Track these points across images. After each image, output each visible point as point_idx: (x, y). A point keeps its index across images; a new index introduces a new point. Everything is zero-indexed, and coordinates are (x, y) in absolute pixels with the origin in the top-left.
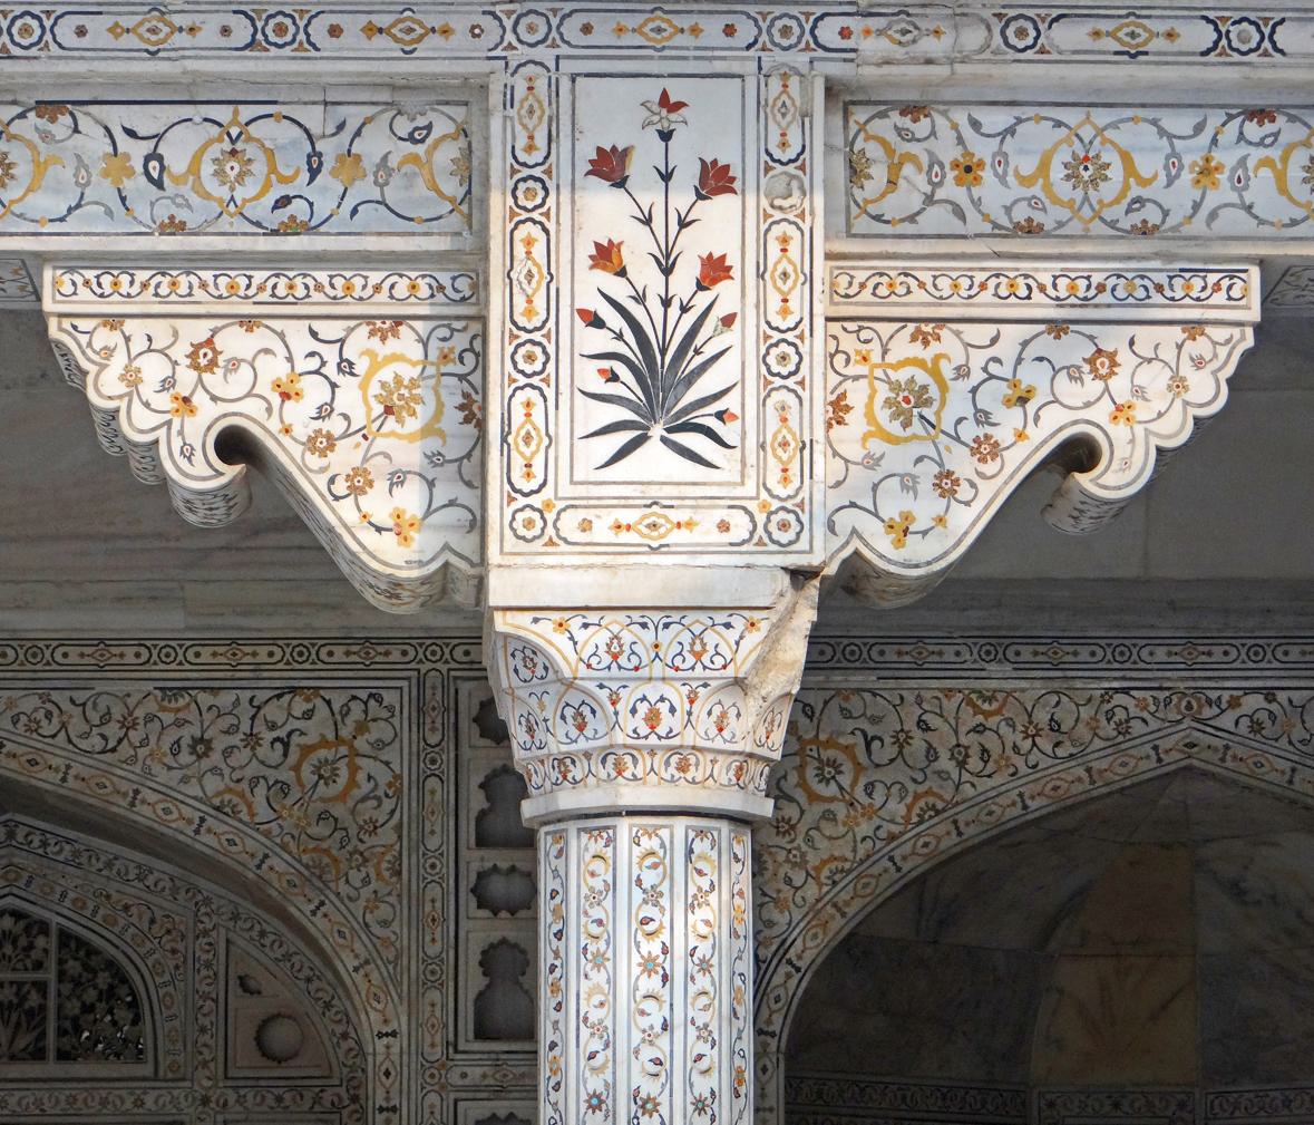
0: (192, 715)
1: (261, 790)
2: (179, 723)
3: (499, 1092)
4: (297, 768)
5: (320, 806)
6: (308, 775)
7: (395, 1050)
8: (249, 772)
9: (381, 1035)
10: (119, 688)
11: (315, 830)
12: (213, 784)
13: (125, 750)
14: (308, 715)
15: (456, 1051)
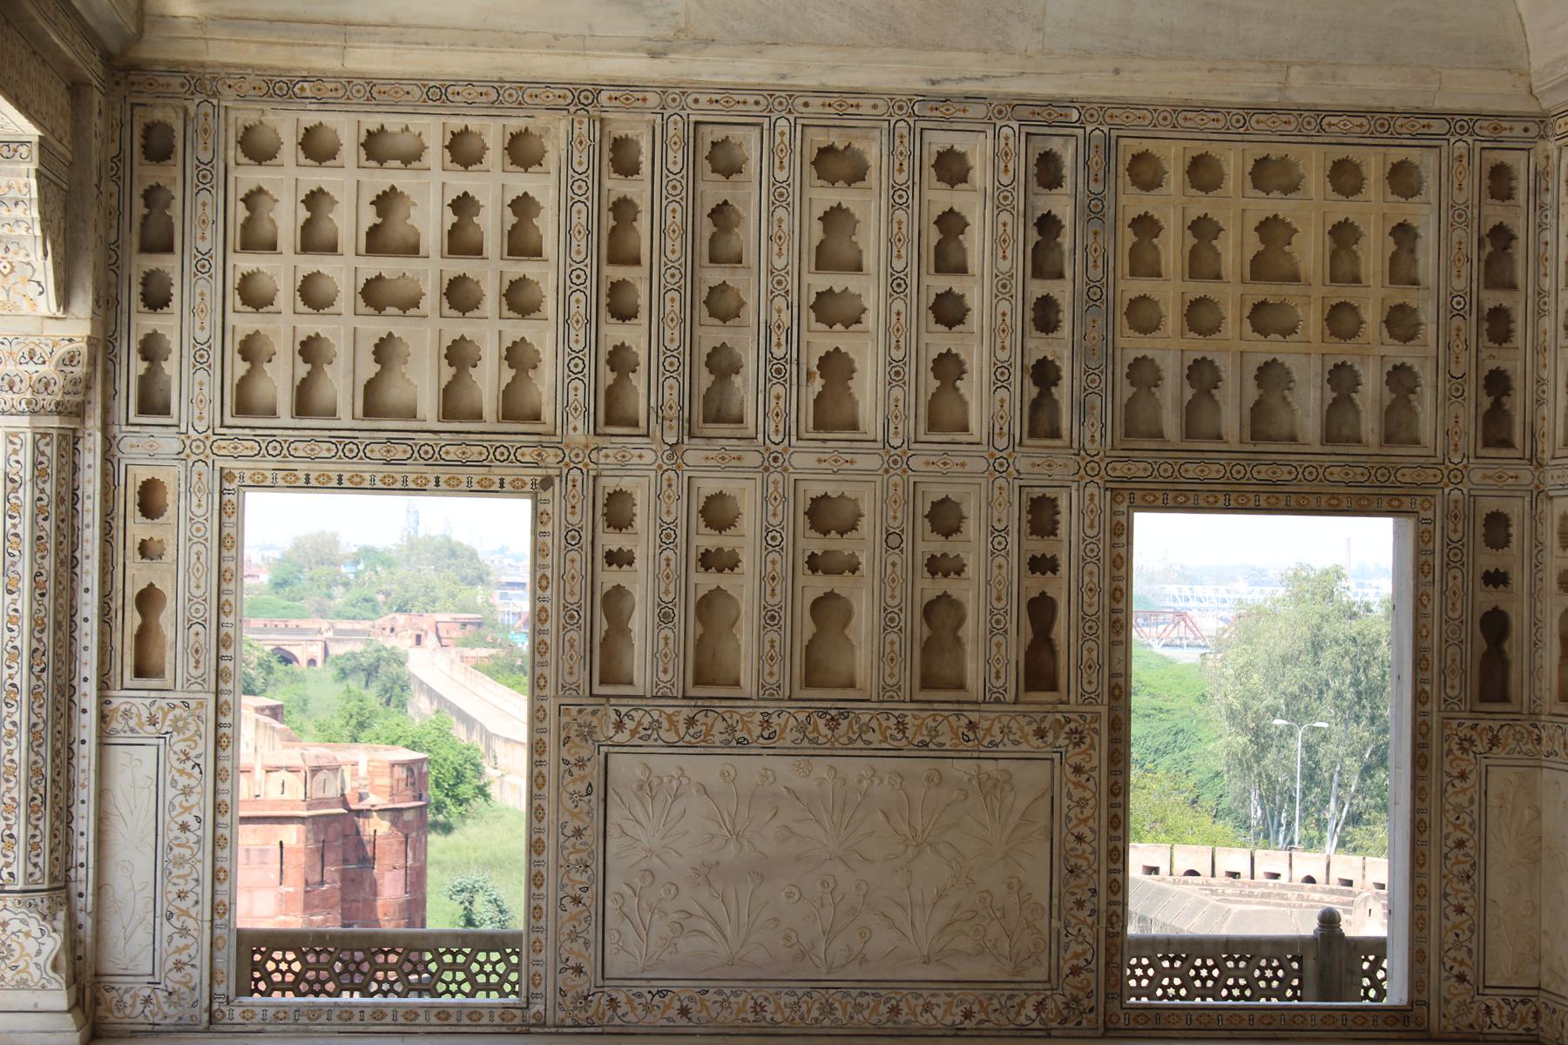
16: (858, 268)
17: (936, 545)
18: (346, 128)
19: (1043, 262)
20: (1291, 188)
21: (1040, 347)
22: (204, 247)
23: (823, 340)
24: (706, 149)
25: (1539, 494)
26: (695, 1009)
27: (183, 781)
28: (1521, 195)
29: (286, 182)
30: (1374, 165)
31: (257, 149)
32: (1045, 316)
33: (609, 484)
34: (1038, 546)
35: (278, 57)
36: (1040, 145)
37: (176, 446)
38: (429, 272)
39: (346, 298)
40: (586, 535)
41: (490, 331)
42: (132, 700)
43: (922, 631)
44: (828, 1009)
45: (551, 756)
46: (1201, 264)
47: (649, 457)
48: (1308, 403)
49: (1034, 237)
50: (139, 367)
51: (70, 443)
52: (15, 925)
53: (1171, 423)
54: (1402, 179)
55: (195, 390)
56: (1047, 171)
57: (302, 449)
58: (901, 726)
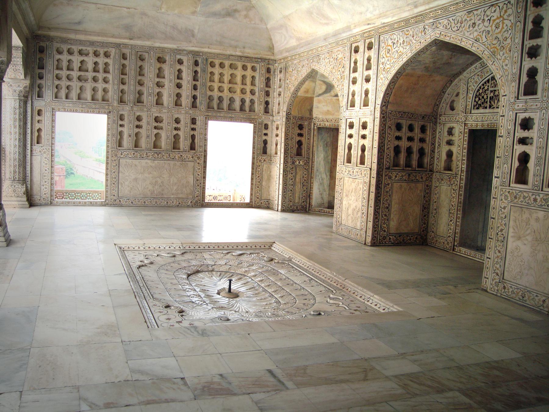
0: (473, 18)
1: (484, 34)
2: (470, 20)
3: (525, 110)
4: (491, 26)
5: (496, 35)
6: (494, 28)
7: (506, 100)
8: (482, 30)
9: (503, 96)
10: (459, 14)
11: (494, 42)
12: (476, 34)
13: (461, 29)
14: (495, 11)
15: (518, 99)
16: (164, 78)
17: (176, 125)
18: (75, 48)
19: (195, 79)
20: (236, 69)
21: (194, 93)
22: (50, 68)
23: (157, 90)
24: (139, 56)
25: (273, 121)
26: (134, 202)
27: (46, 162)
28: (272, 73)
29: (65, 57)
30: (249, 66)
31: (60, 52)
32: (195, 88)
33: (121, 113)
34: (193, 126)
35: (64, 35)
36: (195, 59)
37: (44, 104)
38: (90, 75)
39: (75, 79)
40: (116, 122)
41: (100, 86)
42: (37, 147)
43: (173, 140)
44: (156, 203)
45: (110, 159)
46: (221, 81)
47: (127, 108)
48: (237, 105)
49: (194, 74)
50: (37, 89)
51: (25, 103)
52: (17, 186)
53: (215, 107)
54: (253, 69)
55: (48, 94)
56: (196, 63)
57: (67, 105)
58: (169, 155)
